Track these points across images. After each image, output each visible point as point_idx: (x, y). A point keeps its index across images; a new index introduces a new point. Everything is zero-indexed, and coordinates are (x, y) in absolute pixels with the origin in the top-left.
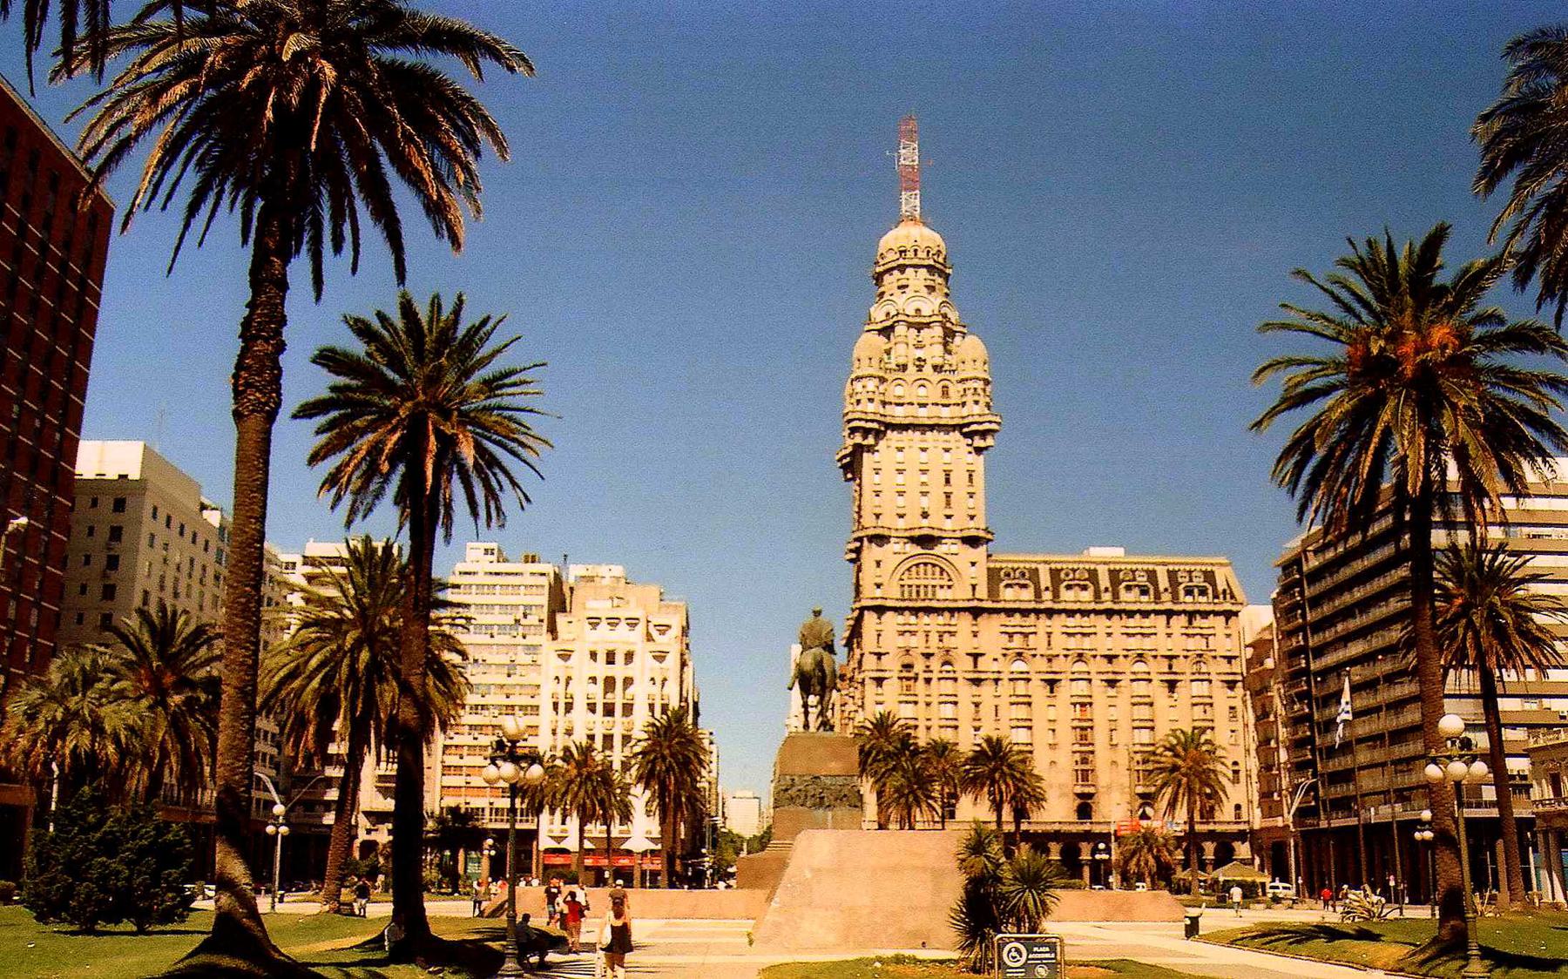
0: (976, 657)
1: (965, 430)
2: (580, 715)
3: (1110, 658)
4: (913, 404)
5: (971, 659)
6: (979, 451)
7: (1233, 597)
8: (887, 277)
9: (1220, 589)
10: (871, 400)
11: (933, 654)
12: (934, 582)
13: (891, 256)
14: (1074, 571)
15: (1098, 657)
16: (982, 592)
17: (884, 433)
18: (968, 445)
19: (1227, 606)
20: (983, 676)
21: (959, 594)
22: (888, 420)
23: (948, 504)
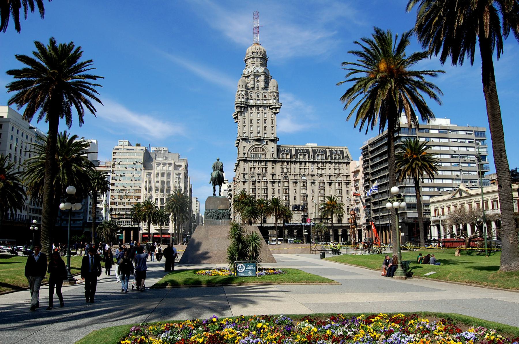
0: (273, 175)
1: (271, 107)
2: (153, 193)
4: (255, 99)
5: (271, 176)
6: (275, 113)
7: (348, 158)
8: (248, 60)
9: (345, 155)
10: (243, 98)
11: (260, 174)
12: (261, 153)
13: (250, 54)
14: (302, 150)
16: (275, 156)
17: (247, 108)
18: (272, 112)
19: (346, 161)
20: (275, 181)
21: (269, 156)
22: (248, 104)
23: (265, 130)
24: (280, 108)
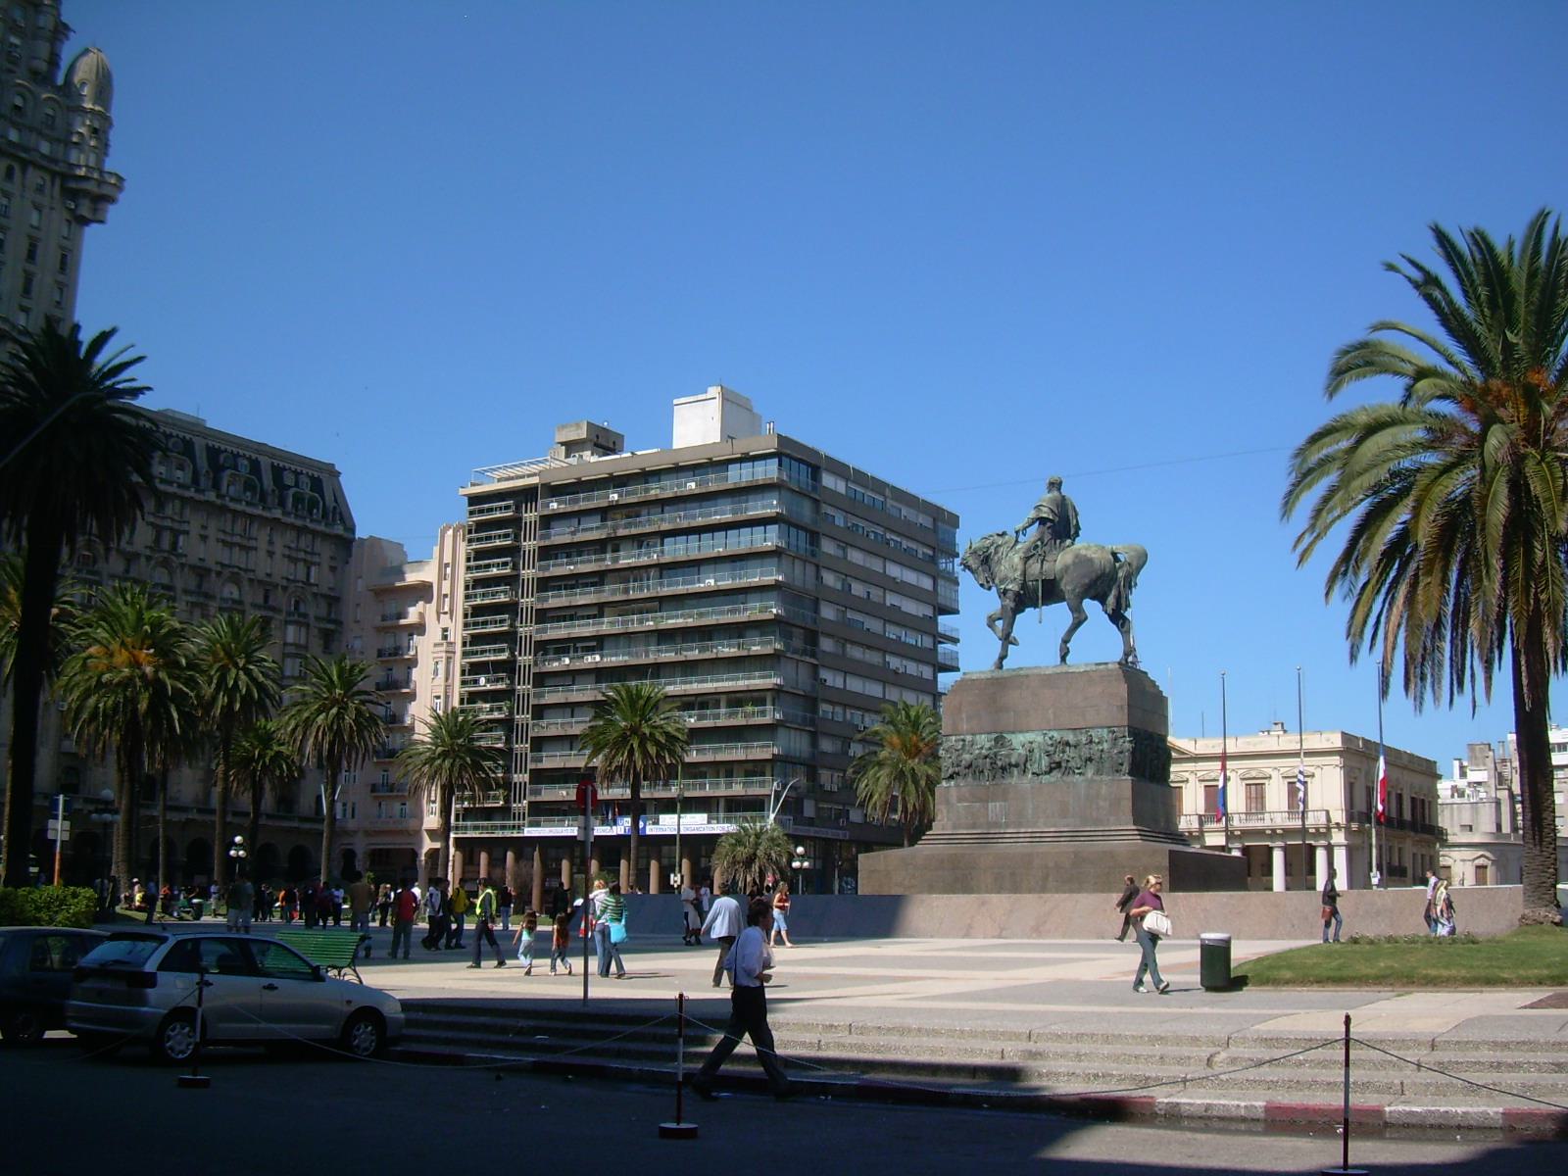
1: (73, 185)
3: (201, 572)
15: (186, 570)
19: (339, 530)
23: (27, 291)
24: (111, 200)
